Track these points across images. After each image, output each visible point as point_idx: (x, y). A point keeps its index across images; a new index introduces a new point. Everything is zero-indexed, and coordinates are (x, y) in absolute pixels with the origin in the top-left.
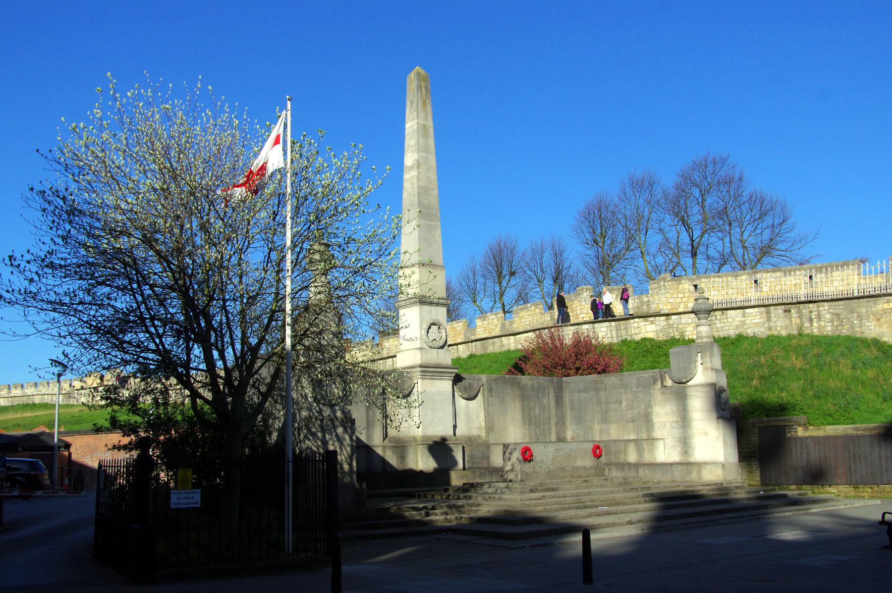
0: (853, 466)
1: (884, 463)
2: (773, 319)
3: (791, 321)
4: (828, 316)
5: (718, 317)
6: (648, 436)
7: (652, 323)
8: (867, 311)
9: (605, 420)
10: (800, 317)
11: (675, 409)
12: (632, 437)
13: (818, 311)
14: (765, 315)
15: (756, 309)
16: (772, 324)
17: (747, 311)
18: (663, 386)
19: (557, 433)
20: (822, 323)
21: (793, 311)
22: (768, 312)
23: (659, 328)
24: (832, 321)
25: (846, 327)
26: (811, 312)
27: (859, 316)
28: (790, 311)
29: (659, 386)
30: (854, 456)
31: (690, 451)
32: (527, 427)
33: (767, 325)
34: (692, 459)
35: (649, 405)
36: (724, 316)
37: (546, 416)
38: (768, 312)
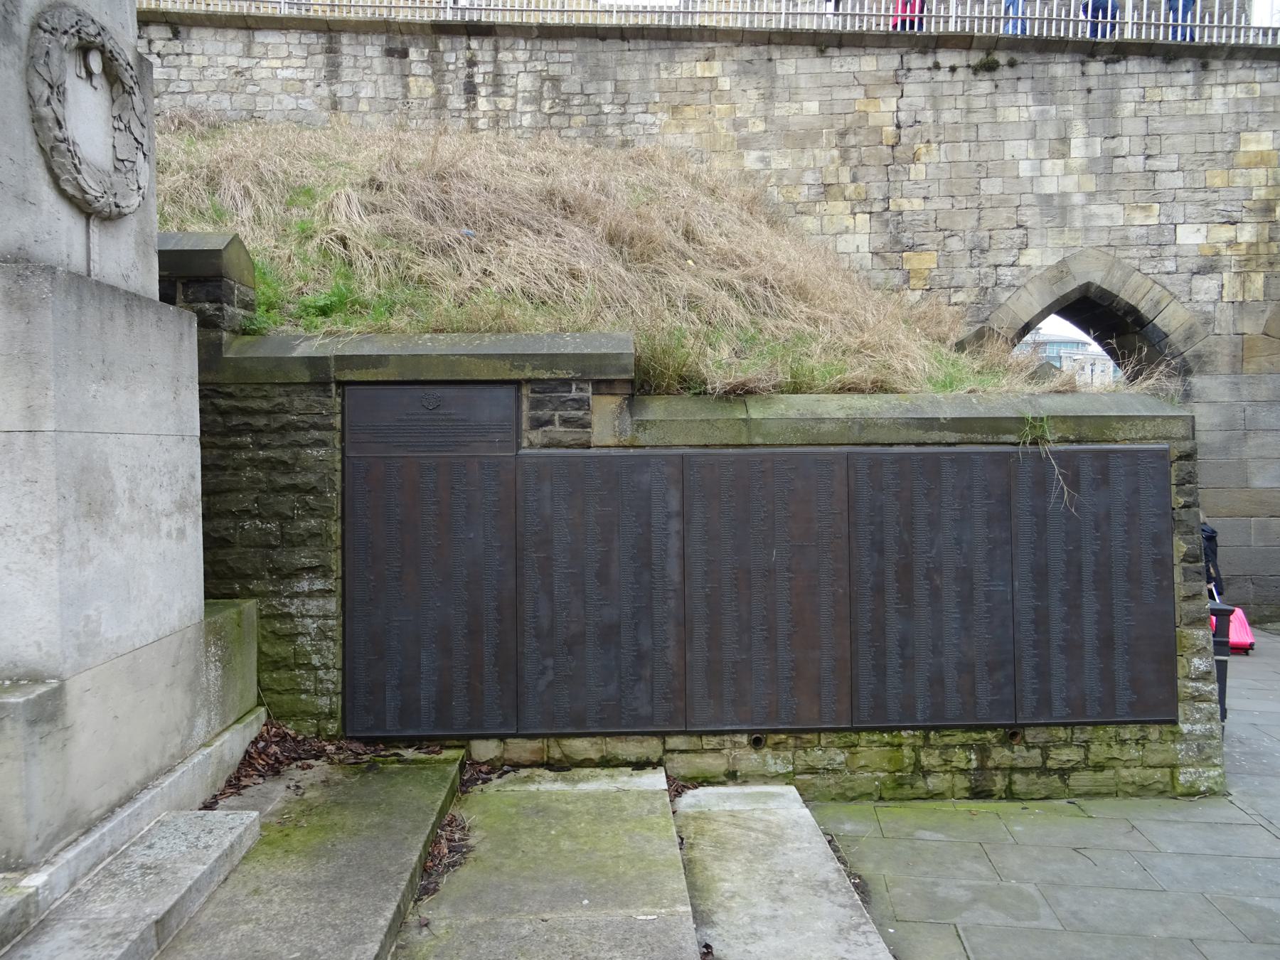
0: (895, 625)
1: (1057, 610)
2: (346, 74)
3: (406, 87)
4: (525, 82)
8: (644, 80)
10: (438, 75)
13: (495, 61)
14: (320, 59)
15: (293, 37)
16: (343, 91)
17: (260, 37)
20: (506, 103)
21: (413, 54)
22: (332, 50)
24: (537, 99)
25: (578, 120)
26: (472, 63)
27: (616, 92)
28: (404, 54)
30: (905, 571)
33: (324, 91)
36: (176, 46)
38: (332, 50)
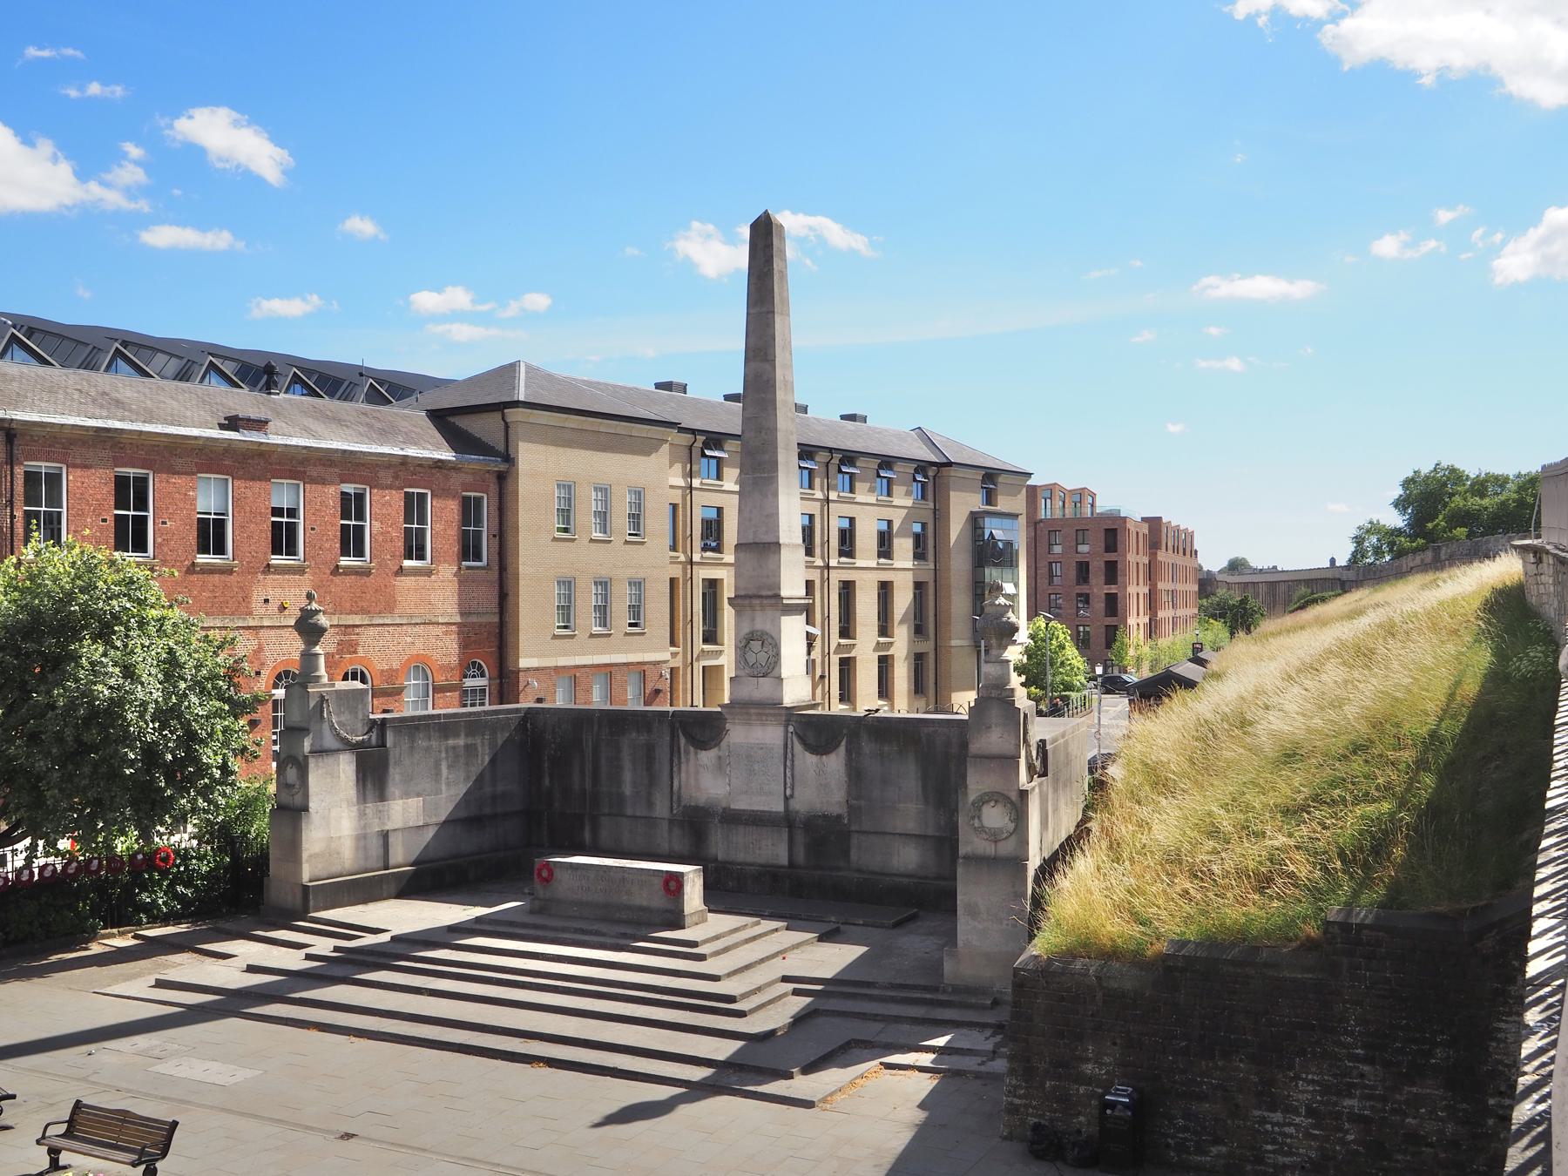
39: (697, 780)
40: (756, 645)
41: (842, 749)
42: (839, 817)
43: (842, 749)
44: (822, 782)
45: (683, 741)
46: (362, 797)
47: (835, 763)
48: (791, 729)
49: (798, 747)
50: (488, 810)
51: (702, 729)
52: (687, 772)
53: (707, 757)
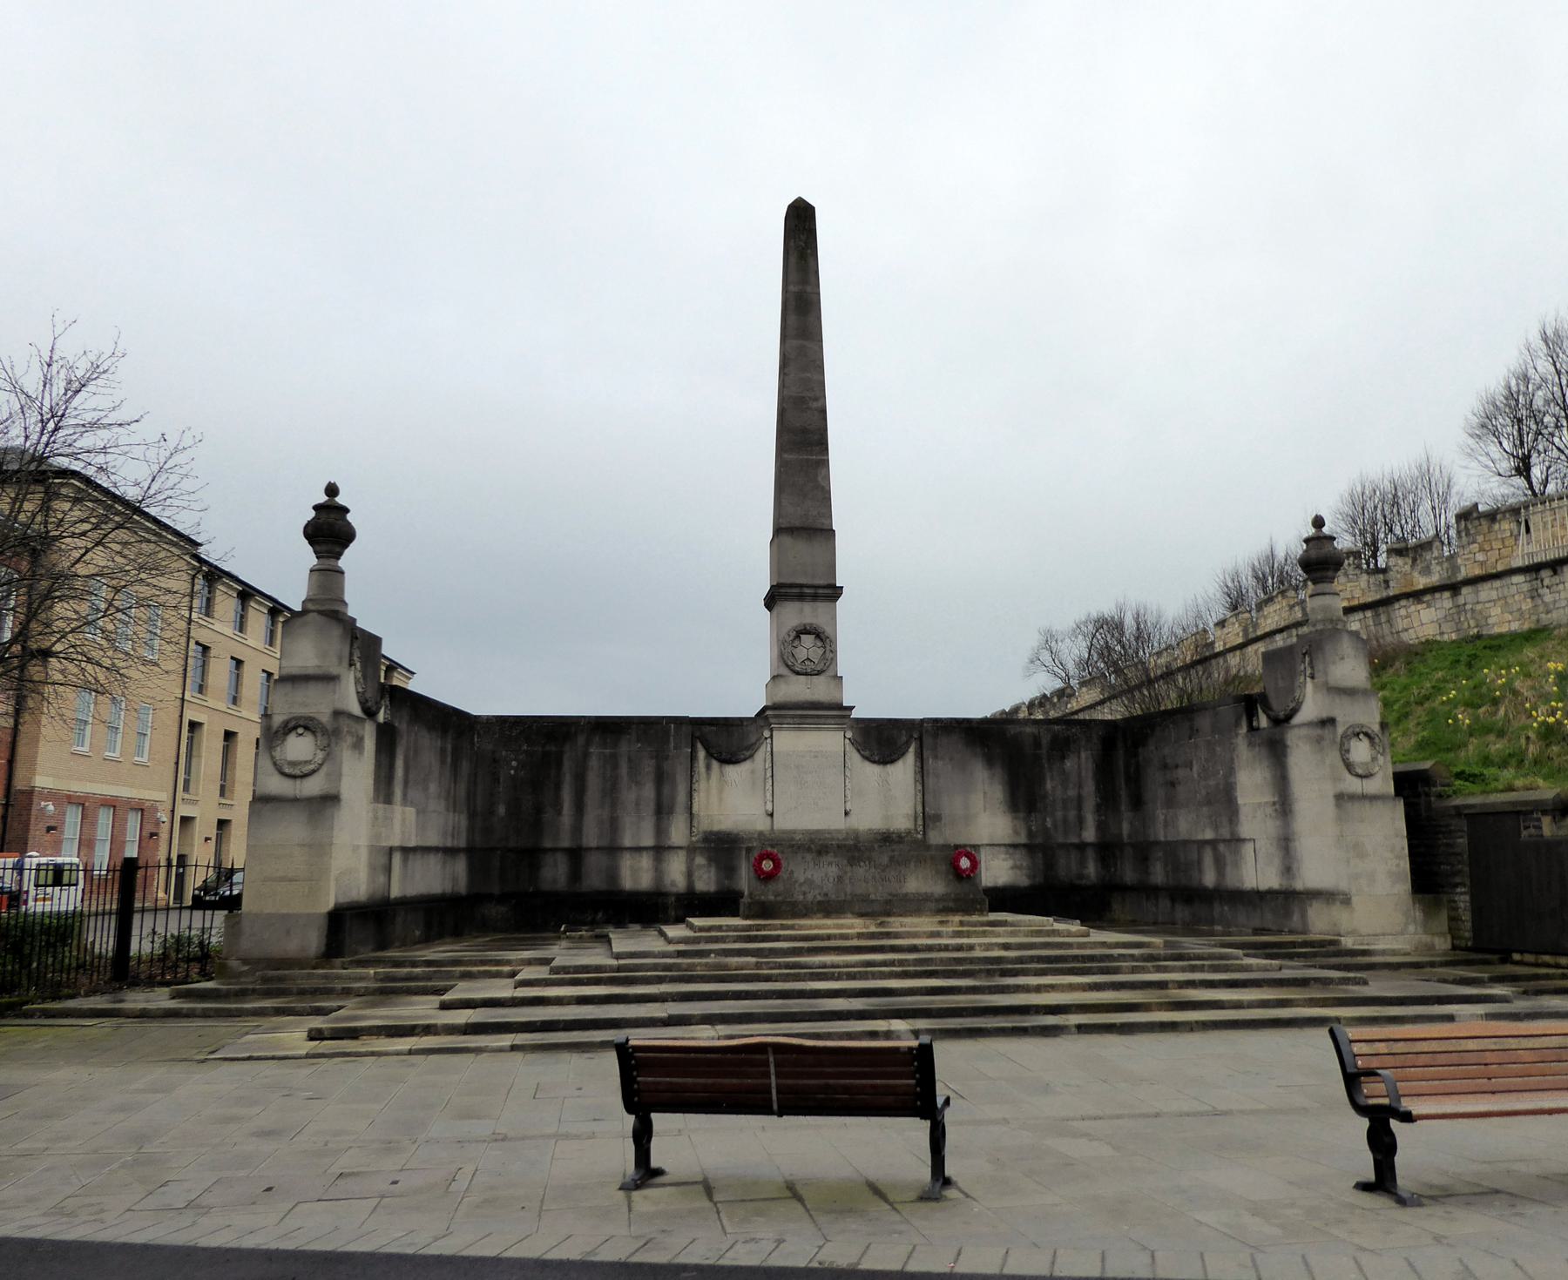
5: (1546, 582)
6: (1232, 833)
7: (1429, 606)
9: (1170, 803)
11: (1268, 775)
12: (1209, 835)
18: (1251, 729)
19: (1101, 827)
23: (1441, 614)
29: (1244, 730)
31: (1295, 866)
32: (1022, 815)
34: (1299, 885)
35: (1231, 771)
37: (1072, 793)
39: (721, 800)
40: (807, 640)
41: (910, 758)
42: (909, 833)
43: (910, 758)
44: (884, 797)
45: (701, 754)
46: (376, 799)
47: (903, 771)
48: (849, 735)
49: (855, 757)
50: (449, 844)
51: (724, 740)
52: (708, 791)
53: (735, 773)
